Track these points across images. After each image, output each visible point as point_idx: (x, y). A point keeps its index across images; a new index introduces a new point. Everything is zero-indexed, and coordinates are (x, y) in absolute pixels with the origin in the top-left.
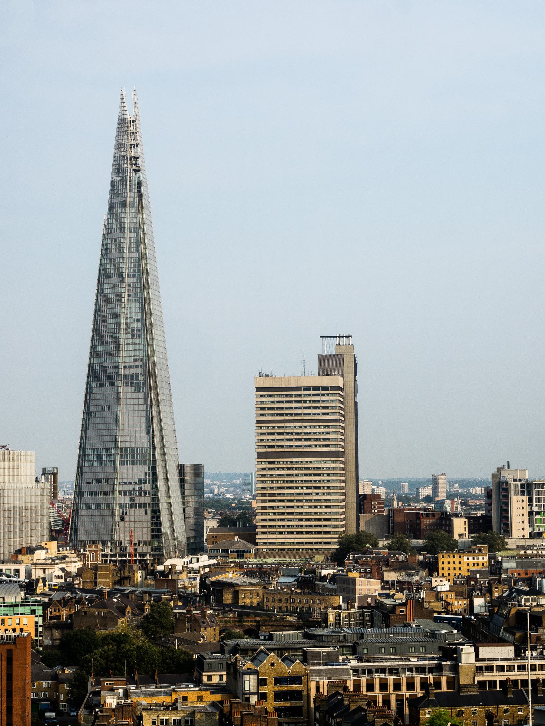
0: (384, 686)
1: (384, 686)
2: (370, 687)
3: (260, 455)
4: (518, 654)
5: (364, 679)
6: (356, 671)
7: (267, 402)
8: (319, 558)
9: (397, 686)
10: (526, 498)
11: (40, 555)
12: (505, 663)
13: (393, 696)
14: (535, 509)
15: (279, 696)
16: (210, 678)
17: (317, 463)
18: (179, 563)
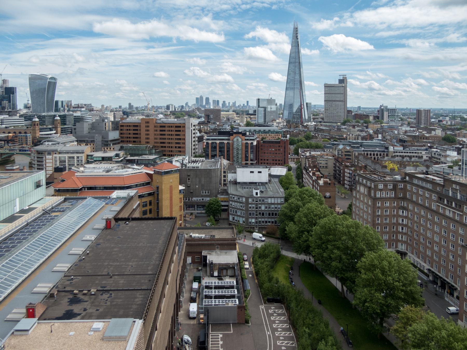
0: (371, 155)
1: (371, 155)
2: (367, 154)
3: (325, 101)
4: (404, 149)
5: (366, 153)
6: (364, 151)
7: (327, 89)
8: (339, 124)
9: (374, 155)
10: (387, 112)
11: (278, 121)
12: (401, 151)
13: (376, 157)
14: (390, 115)
15: (346, 155)
16: (330, 150)
17: (338, 103)
18: (309, 123)
